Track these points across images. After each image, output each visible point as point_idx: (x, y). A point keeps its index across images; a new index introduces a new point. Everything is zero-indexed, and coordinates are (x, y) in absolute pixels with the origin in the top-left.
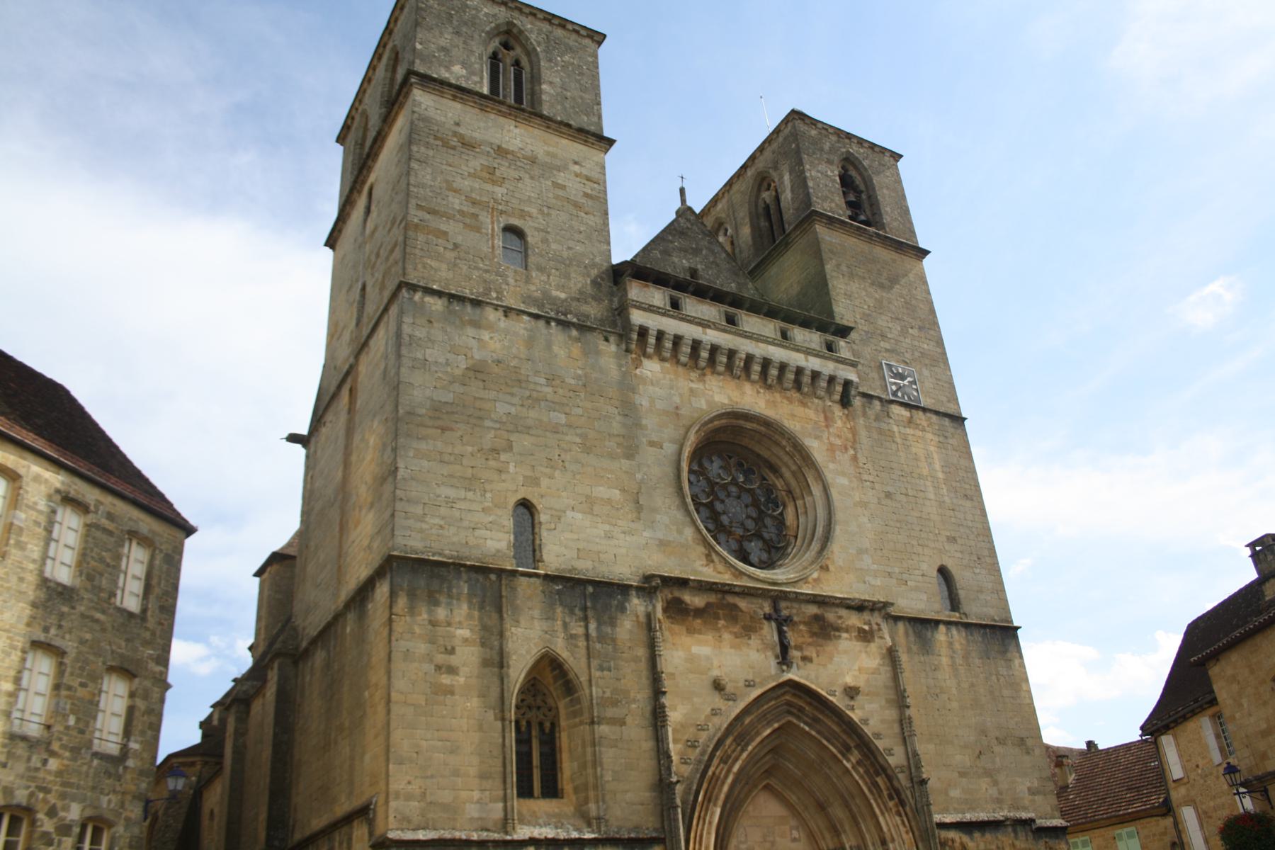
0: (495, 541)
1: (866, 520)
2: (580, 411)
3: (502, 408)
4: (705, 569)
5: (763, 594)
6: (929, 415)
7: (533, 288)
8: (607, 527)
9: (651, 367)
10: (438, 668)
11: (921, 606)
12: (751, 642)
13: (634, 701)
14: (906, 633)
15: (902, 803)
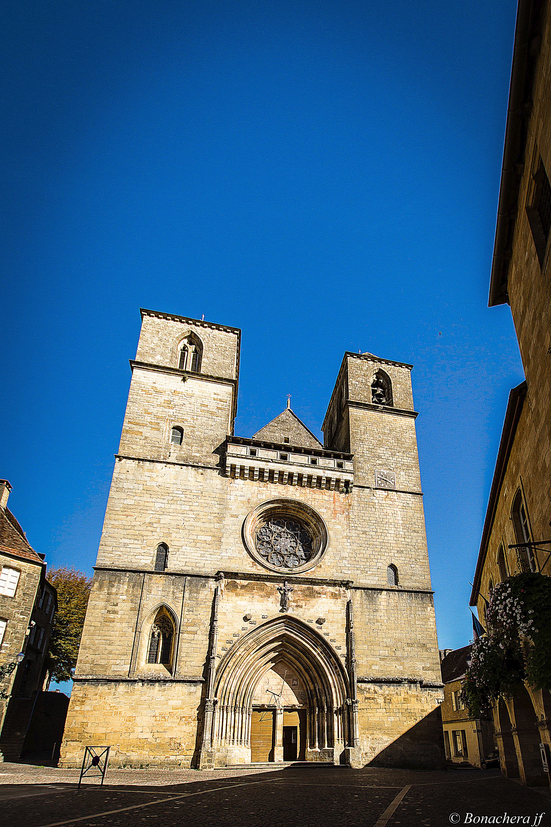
8: (202, 552)
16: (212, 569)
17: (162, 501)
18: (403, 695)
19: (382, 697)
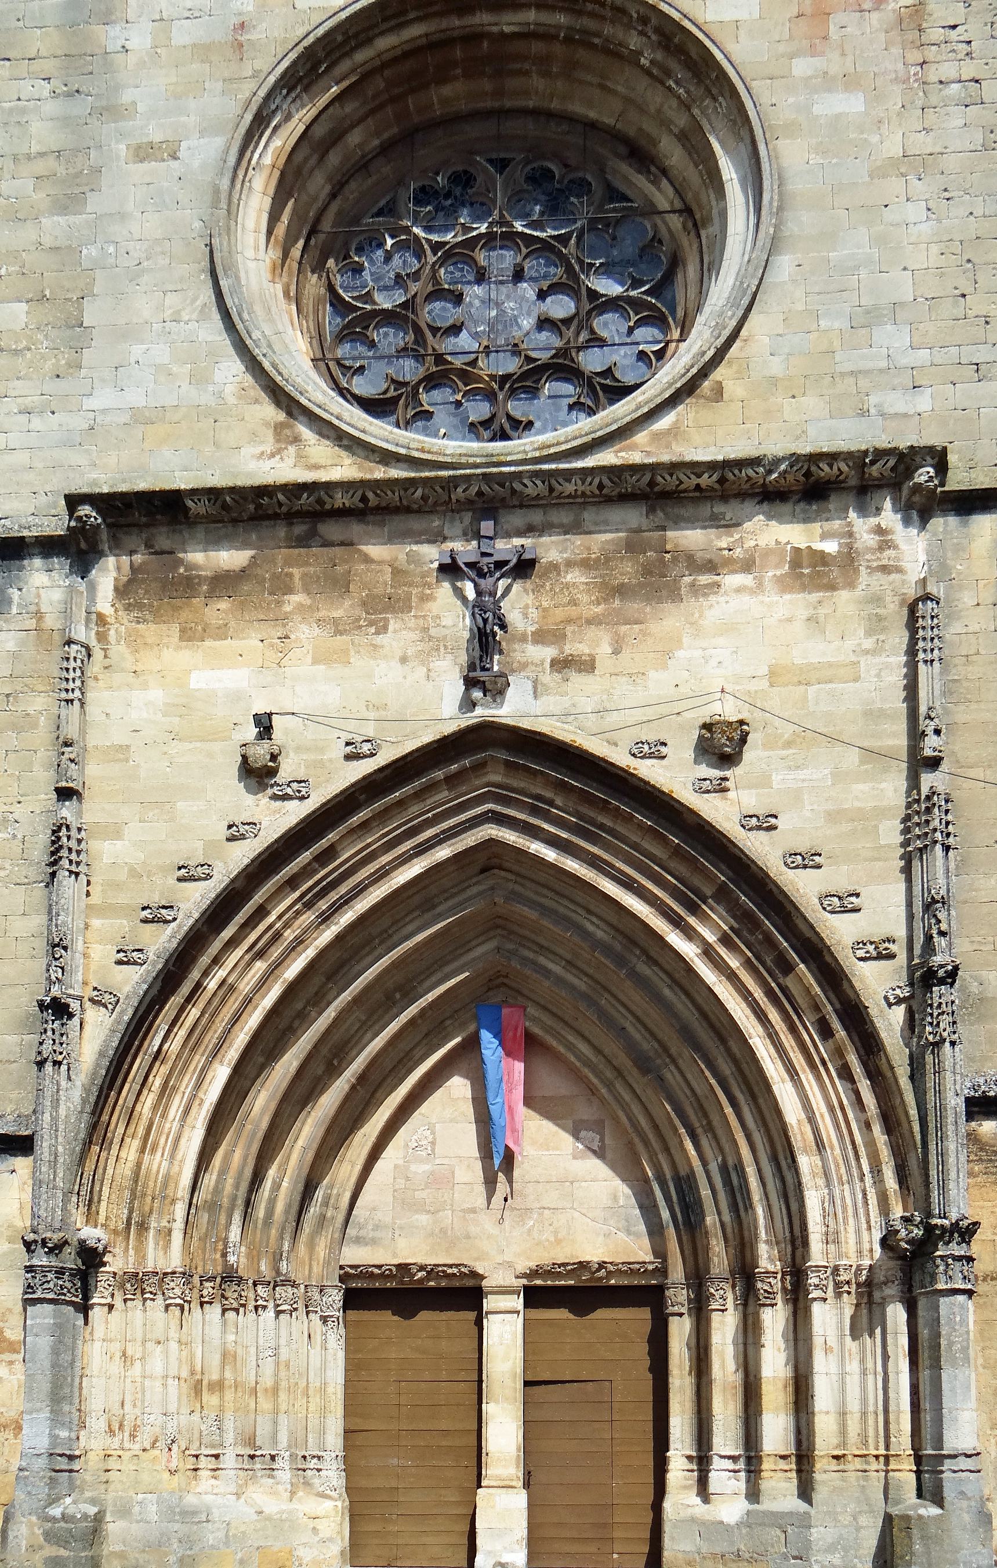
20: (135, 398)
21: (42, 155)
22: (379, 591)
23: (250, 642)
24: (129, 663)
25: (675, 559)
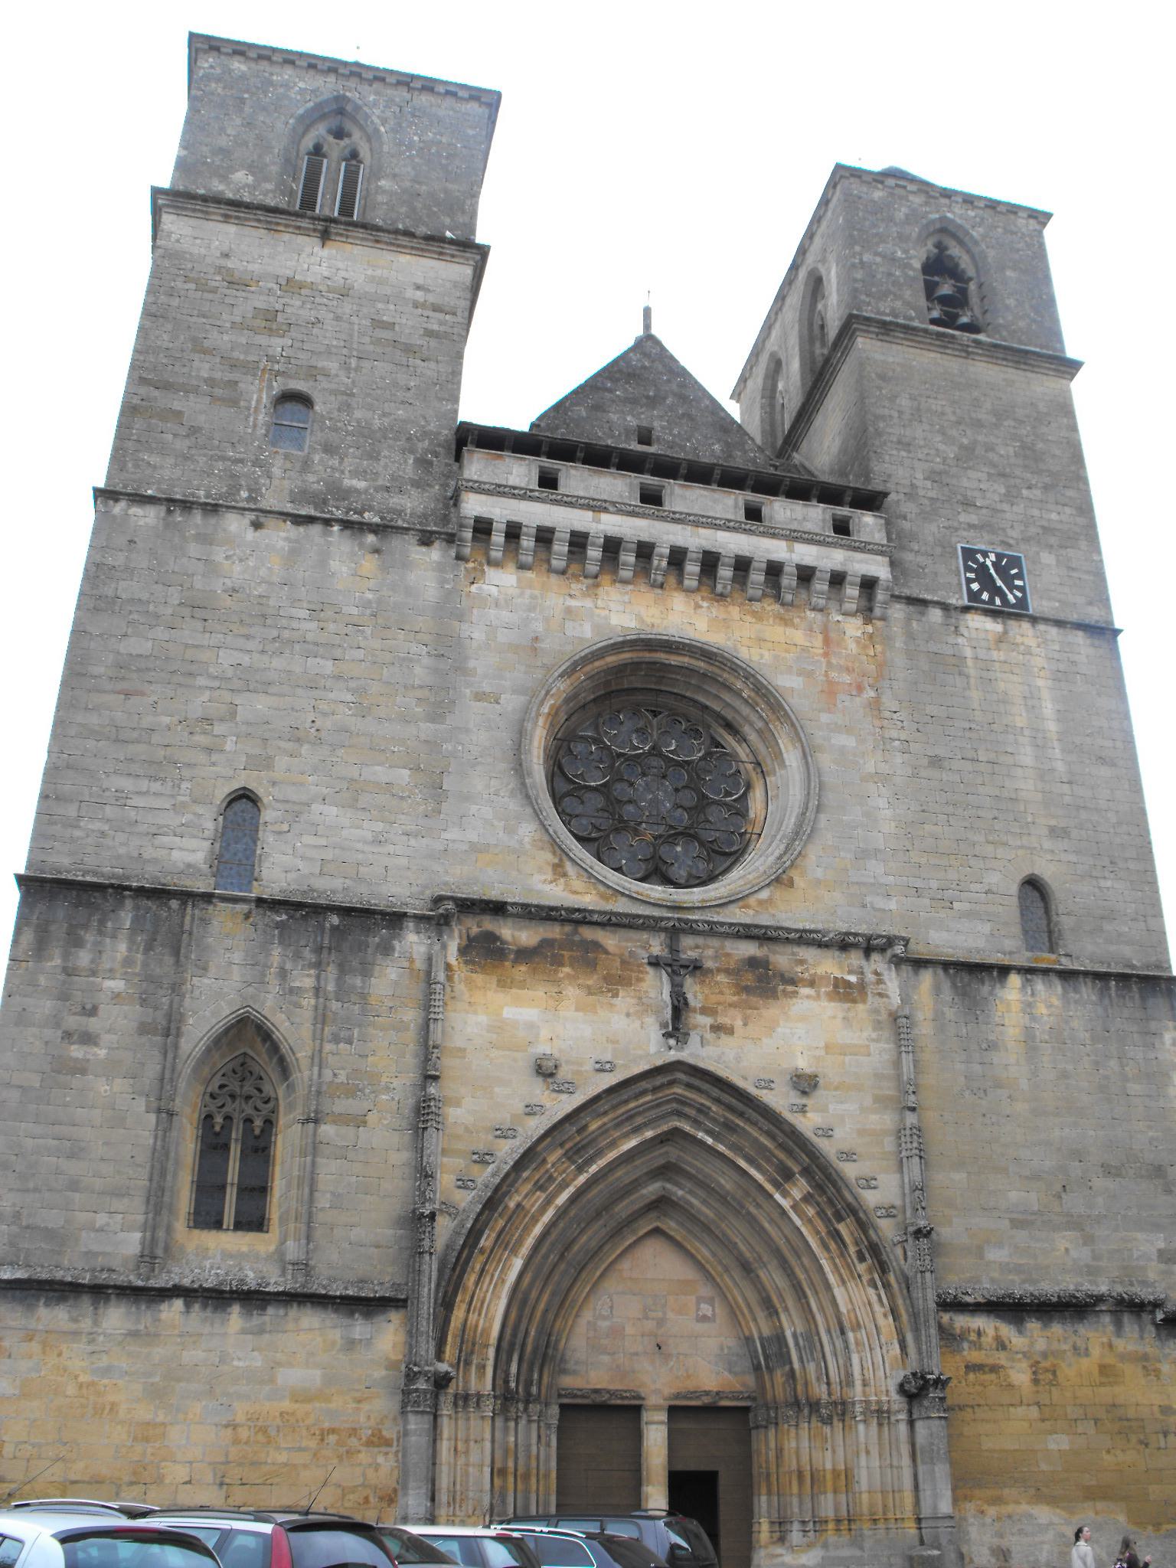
0: (186, 853)
1: (882, 803)
2: (359, 654)
3: (227, 658)
4: (547, 888)
5: (648, 925)
6: (1042, 627)
7: (311, 478)
9: (502, 581)
10: (68, 1035)
11: (981, 943)
12: (617, 1001)
13: (388, 1089)
14: (937, 990)
15: (883, 1268)
16: (415, 889)
17: (241, 642)
18: (1096, 1352)
19: (1025, 1365)
20: (473, 836)
21: (421, 687)
22: (613, 972)
23: (539, 993)
24: (466, 996)
25: (774, 975)
